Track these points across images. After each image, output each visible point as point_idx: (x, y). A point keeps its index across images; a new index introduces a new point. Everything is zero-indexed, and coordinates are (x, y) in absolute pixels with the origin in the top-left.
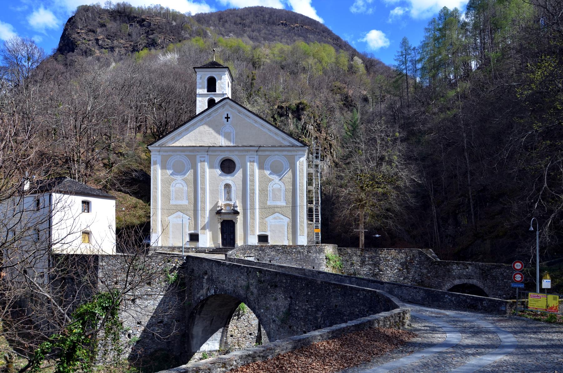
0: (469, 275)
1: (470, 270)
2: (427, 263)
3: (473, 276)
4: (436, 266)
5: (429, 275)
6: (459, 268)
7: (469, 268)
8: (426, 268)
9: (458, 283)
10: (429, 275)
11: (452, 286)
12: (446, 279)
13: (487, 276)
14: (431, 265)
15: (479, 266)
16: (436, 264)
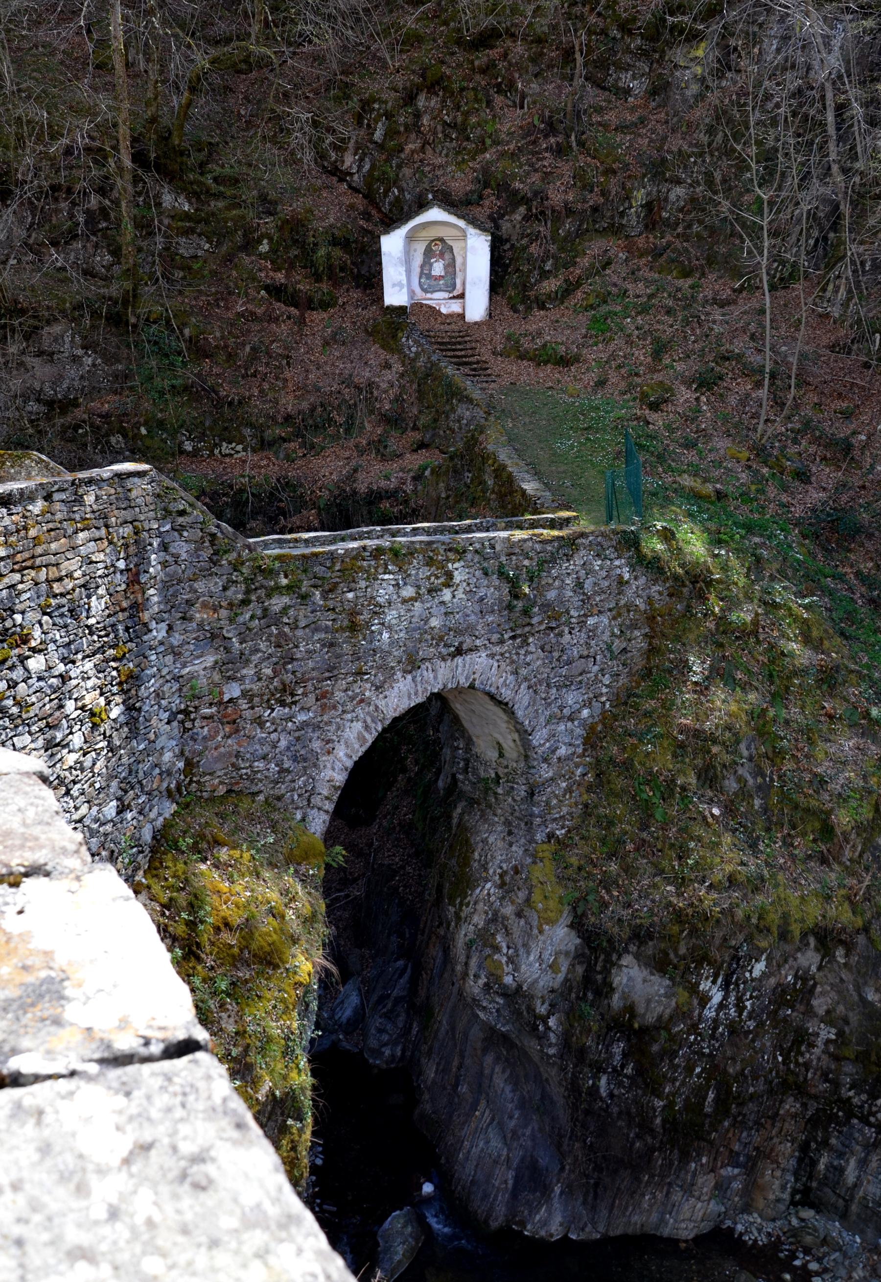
0: (458, 632)
1: (460, 594)
2: (215, 584)
3: (470, 630)
4: (277, 603)
5: (233, 691)
6: (408, 592)
7: (458, 577)
8: (215, 637)
9: (406, 704)
10: (233, 691)
11: (370, 739)
12: (339, 695)
13: (526, 612)
14: (245, 602)
15: (496, 556)
16: (278, 589)
